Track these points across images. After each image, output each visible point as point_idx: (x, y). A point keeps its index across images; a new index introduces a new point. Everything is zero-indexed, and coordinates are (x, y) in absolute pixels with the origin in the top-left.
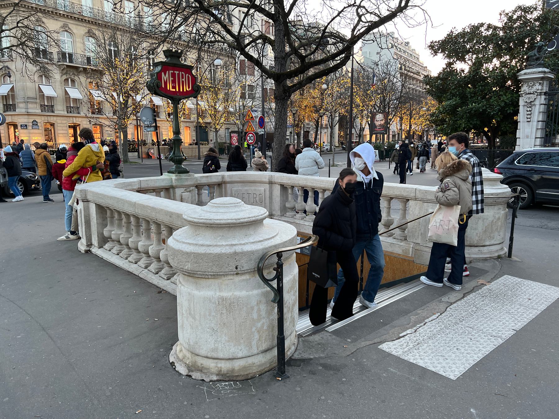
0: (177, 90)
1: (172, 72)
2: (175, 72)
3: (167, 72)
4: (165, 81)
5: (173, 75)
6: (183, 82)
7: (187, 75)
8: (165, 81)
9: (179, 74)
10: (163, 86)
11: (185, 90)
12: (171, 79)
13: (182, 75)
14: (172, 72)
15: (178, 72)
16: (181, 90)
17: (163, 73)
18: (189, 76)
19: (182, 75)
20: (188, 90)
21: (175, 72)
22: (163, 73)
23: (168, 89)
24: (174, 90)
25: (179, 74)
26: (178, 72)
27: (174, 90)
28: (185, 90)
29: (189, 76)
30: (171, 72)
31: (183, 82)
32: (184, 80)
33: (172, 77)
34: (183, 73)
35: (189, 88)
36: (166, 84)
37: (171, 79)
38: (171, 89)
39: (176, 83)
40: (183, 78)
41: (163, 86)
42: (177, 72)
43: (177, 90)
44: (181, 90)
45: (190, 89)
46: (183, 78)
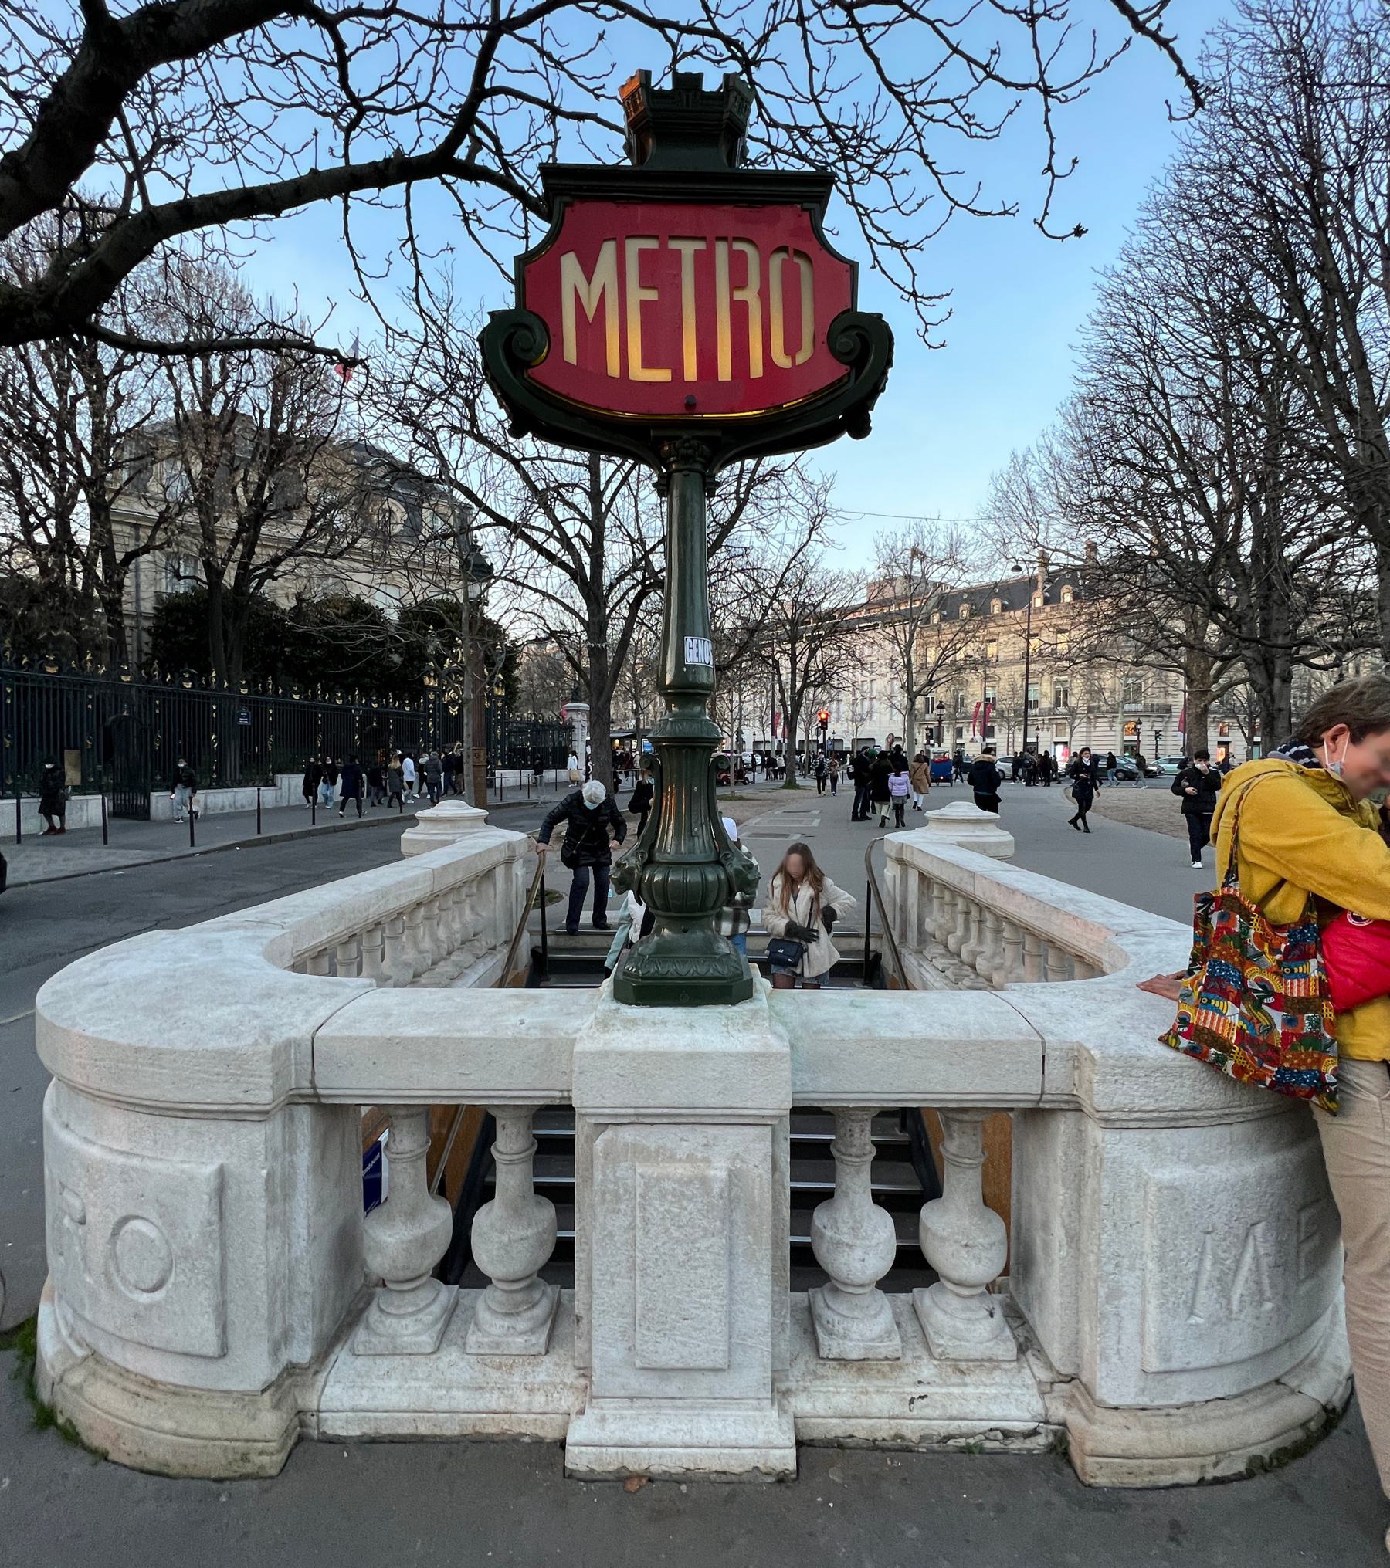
1: (652, 244)
3: (608, 250)
4: (590, 314)
6: (739, 311)
8: (590, 314)
9: (705, 265)
10: (571, 354)
11: (756, 370)
13: (738, 264)
14: (652, 244)
15: (701, 246)
16: (725, 372)
17: (570, 265)
19: (738, 264)
20: (781, 360)
21: (674, 245)
22: (570, 265)
23: (614, 369)
24: (663, 375)
25: (705, 265)
27: (663, 375)
28: (756, 370)
30: (633, 247)
31: (739, 311)
32: (749, 294)
33: (644, 285)
34: (738, 246)
36: (591, 330)
37: (637, 295)
38: (638, 373)
40: (738, 281)
41: (571, 354)
42: (688, 249)
43: (691, 373)
44: (725, 372)
46: (738, 281)
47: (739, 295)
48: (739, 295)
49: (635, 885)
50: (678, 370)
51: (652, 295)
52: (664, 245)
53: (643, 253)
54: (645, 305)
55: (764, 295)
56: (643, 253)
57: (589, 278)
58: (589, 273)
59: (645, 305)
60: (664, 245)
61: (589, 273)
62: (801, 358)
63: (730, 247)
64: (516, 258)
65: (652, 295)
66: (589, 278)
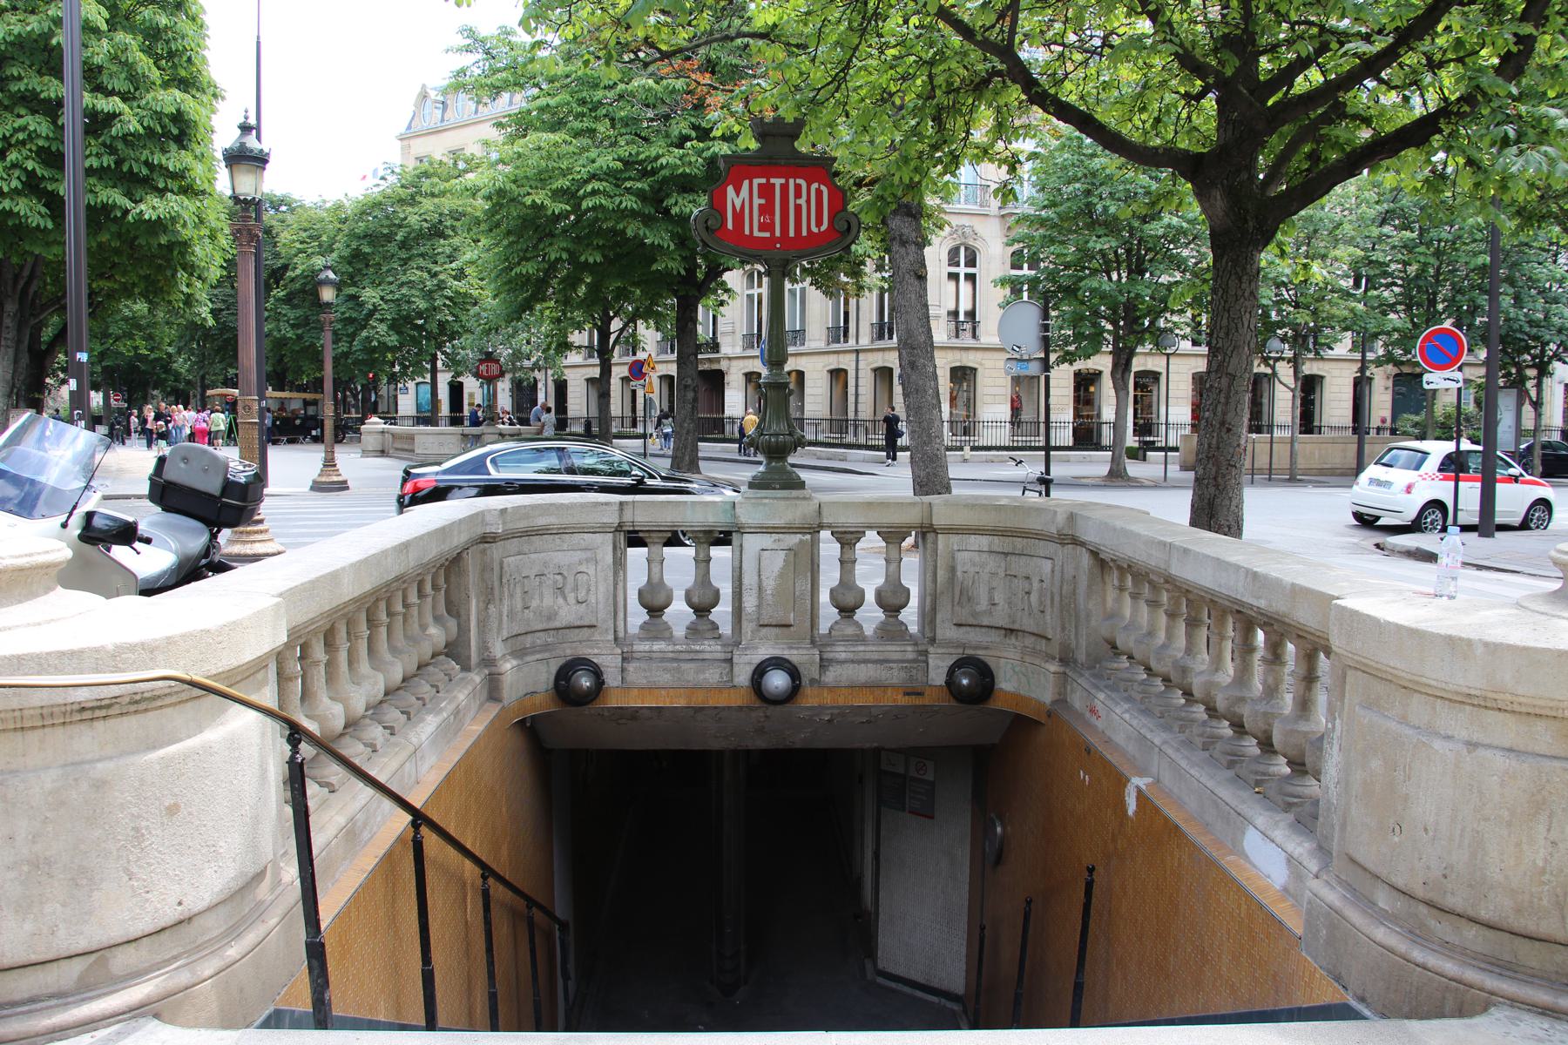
0: (778, 234)
1: (763, 181)
2: (772, 181)
3: (746, 183)
4: (738, 208)
5: (767, 191)
6: (798, 208)
7: (815, 186)
8: (738, 208)
9: (785, 188)
10: (730, 226)
11: (804, 233)
12: (757, 201)
13: (798, 188)
14: (763, 181)
15: (783, 181)
16: (792, 234)
18: (823, 188)
19: (798, 188)
20: (814, 229)
21: (772, 181)
23: (747, 232)
24: (767, 235)
25: (785, 188)
26: (783, 181)
27: (767, 235)
28: (804, 233)
29: (823, 188)
30: (756, 181)
31: (798, 208)
32: (802, 201)
33: (760, 197)
34: (798, 181)
35: (819, 223)
36: (739, 217)
37: (757, 201)
38: (756, 233)
39: (772, 214)
40: (798, 195)
41: (730, 226)
42: (778, 182)
43: (778, 234)
44: (792, 234)
45: (824, 228)
46: (798, 195)
47: (798, 201)
48: (798, 201)
50: (773, 233)
51: (763, 201)
52: (768, 181)
53: (760, 185)
55: (808, 201)
56: (760, 185)
57: (738, 195)
58: (738, 193)
60: (768, 181)
61: (738, 193)
65: (763, 201)
66: (738, 195)
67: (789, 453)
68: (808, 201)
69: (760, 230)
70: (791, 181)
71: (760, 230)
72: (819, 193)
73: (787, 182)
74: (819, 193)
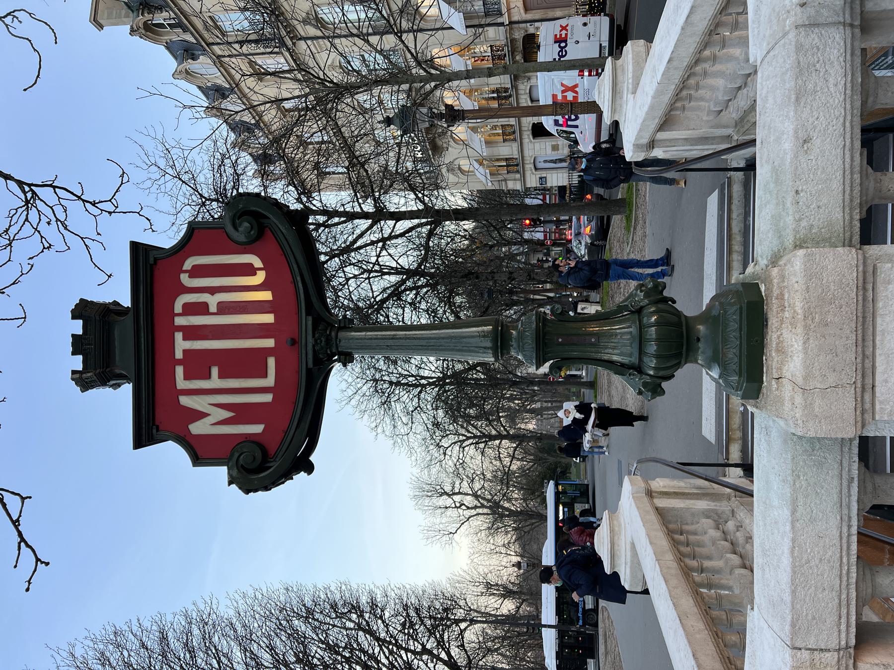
0: (270, 343)
1: (180, 371)
2: (179, 355)
3: (184, 400)
4: (227, 414)
6: (225, 308)
7: (185, 279)
8: (227, 414)
9: (191, 333)
10: (257, 429)
11: (266, 296)
12: (215, 381)
13: (191, 309)
14: (180, 371)
15: (179, 336)
16: (269, 318)
17: (197, 428)
19: (191, 309)
20: (260, 278)
21: (179, 355)
22: (197, 428)
23: (268, 398)
24: (271, 362)
25: (191, 333)
26: (179, 336)
27: (271, 362)
28: (266, 296)
29: (188, 264)
30: (181, 383)
31: (225, 308)
32: (213, 301)
33: (208, 376)
34: (178, 308)
35: (250, 270)
36: (241, 414)
37: (215, 381)
40: (202, 309)
41: (257, 429)
42: (181, 345)
43: (270, 343)
44: (268, 318)
46: (202, 309)
47: (213, 308)
48: (213, 308)
49: (658, 381)
50: (267, 352)
51: (215, 371)
52: (179, 362)
53: (187, 377)
54: (221, 376)
55: (213, 291)
56: (187, 377)
57: (205, 415)
58: (201, 415)
59: (221, 376)
60: (179, 362)
61: (200, 415)
62: (257, 263)
63: (179, 315)
64: (194, 466)
65: (215, 371)
66: (205, 415)
67: (678, 314)
68: (213, 291)
69: (265, 375)
70: (179, 321)
71: (265, 375)
72: (198, 271)
73: (181, 328)
74: (198, 271)
